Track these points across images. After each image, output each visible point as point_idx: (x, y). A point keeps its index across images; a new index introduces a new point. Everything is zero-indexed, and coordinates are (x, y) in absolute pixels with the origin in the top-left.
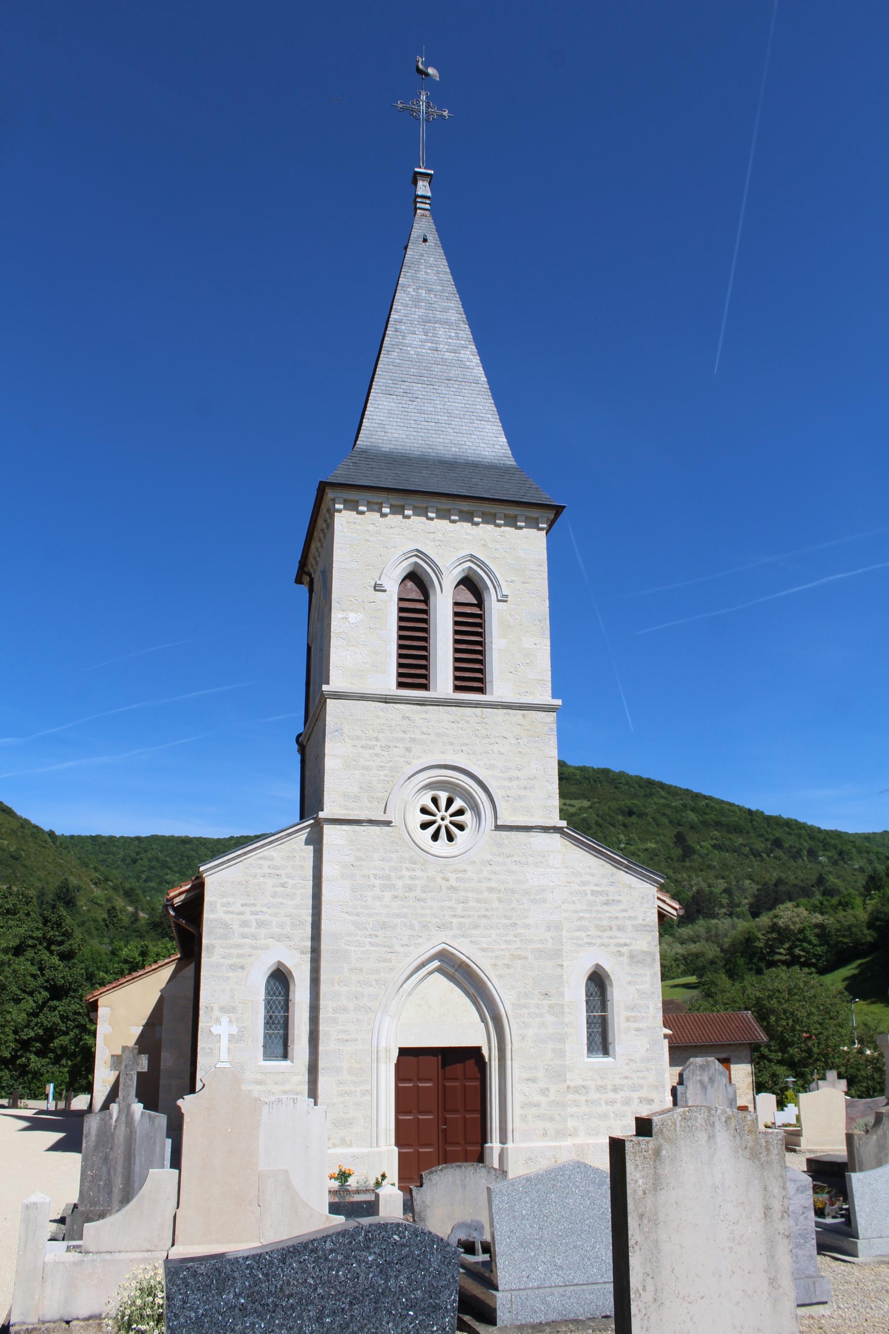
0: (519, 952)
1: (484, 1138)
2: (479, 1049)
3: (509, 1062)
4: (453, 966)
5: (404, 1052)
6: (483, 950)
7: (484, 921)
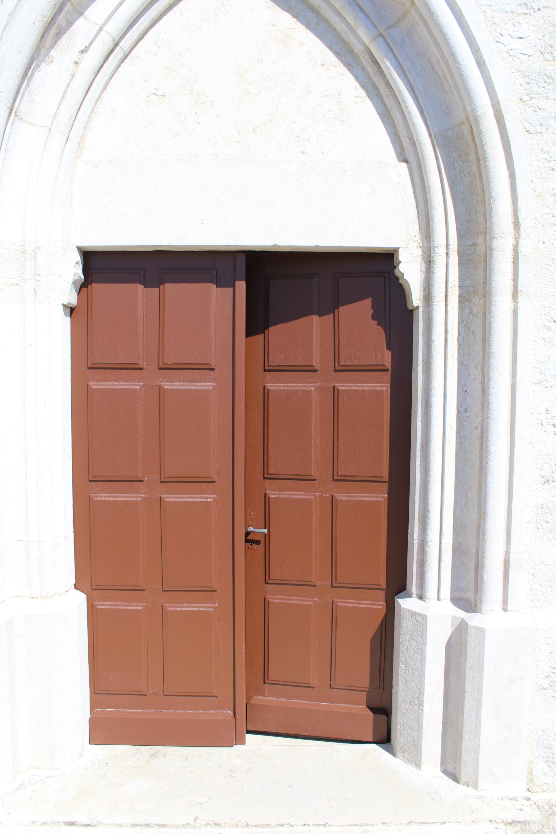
1: (397, 582)
2: (386, 260)
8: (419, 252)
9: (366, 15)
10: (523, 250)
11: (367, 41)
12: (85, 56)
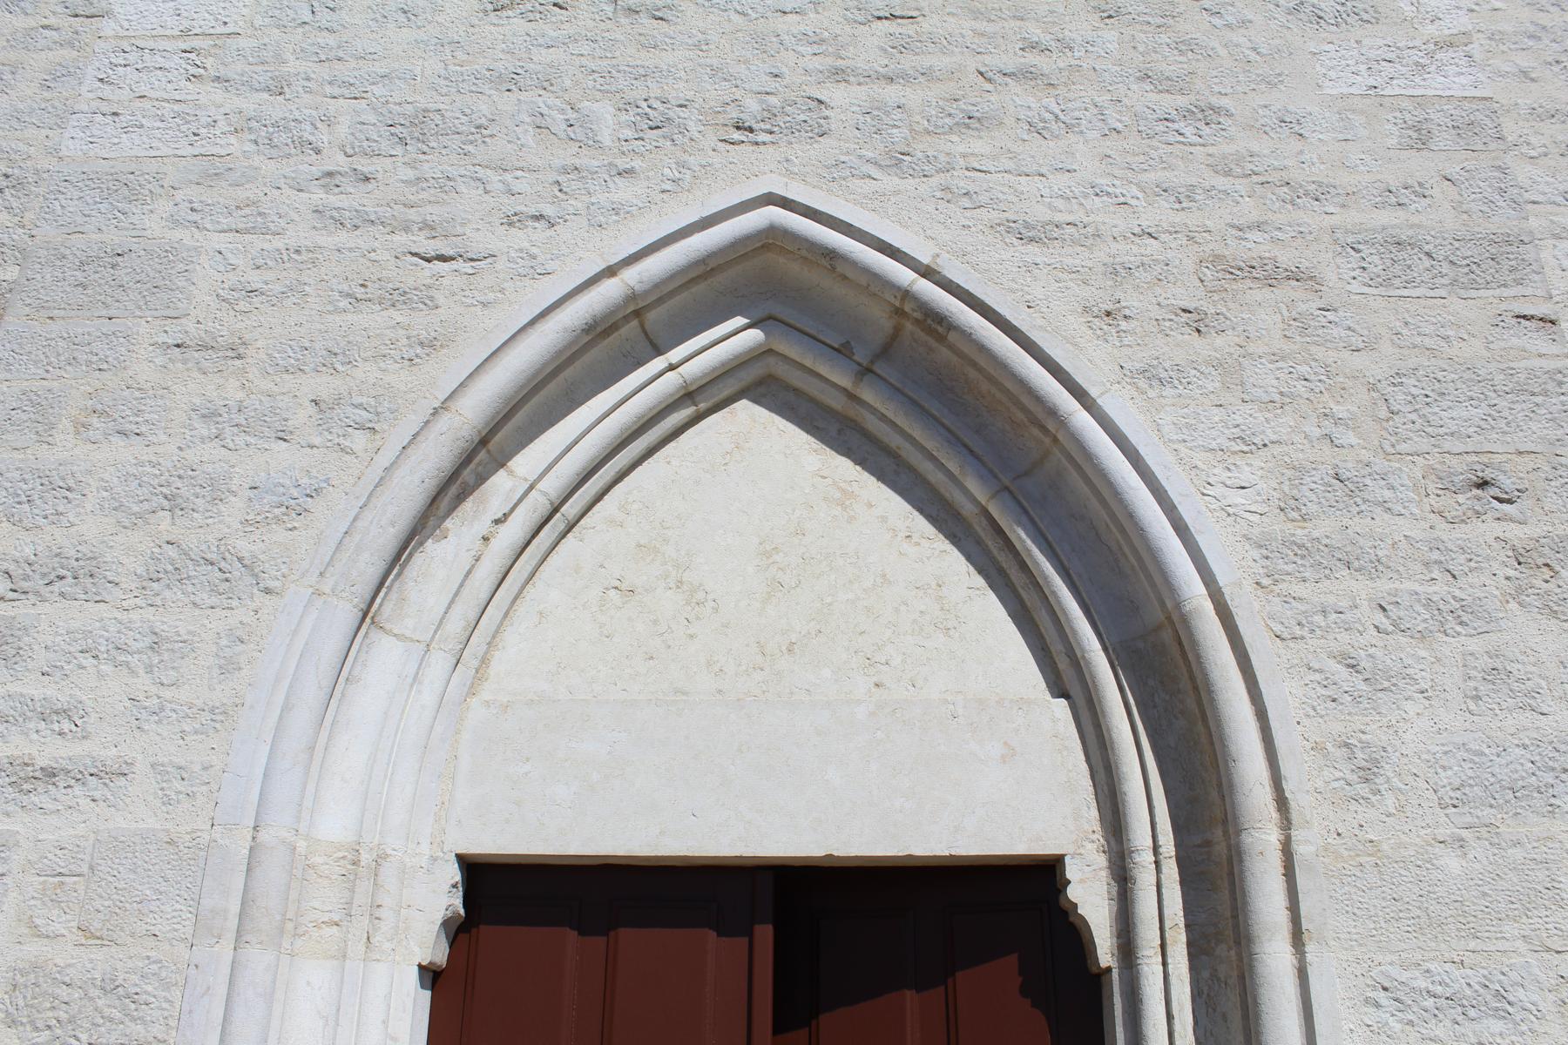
0: (1257, 246)
3: (1275, 957)
4: (843, 351)
5: (501, 894)
6: (1028, 234)
7: (1021, 99)
8: (1102, 861)
9: (977, 457)
10: (1301, 850)
11: (982, 499)
12: (502, 528)
